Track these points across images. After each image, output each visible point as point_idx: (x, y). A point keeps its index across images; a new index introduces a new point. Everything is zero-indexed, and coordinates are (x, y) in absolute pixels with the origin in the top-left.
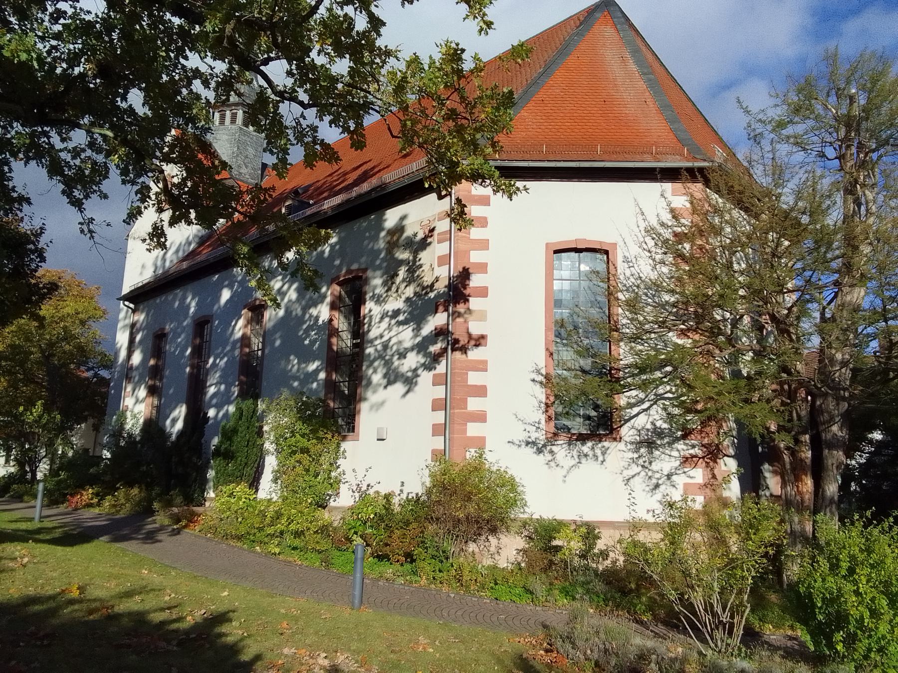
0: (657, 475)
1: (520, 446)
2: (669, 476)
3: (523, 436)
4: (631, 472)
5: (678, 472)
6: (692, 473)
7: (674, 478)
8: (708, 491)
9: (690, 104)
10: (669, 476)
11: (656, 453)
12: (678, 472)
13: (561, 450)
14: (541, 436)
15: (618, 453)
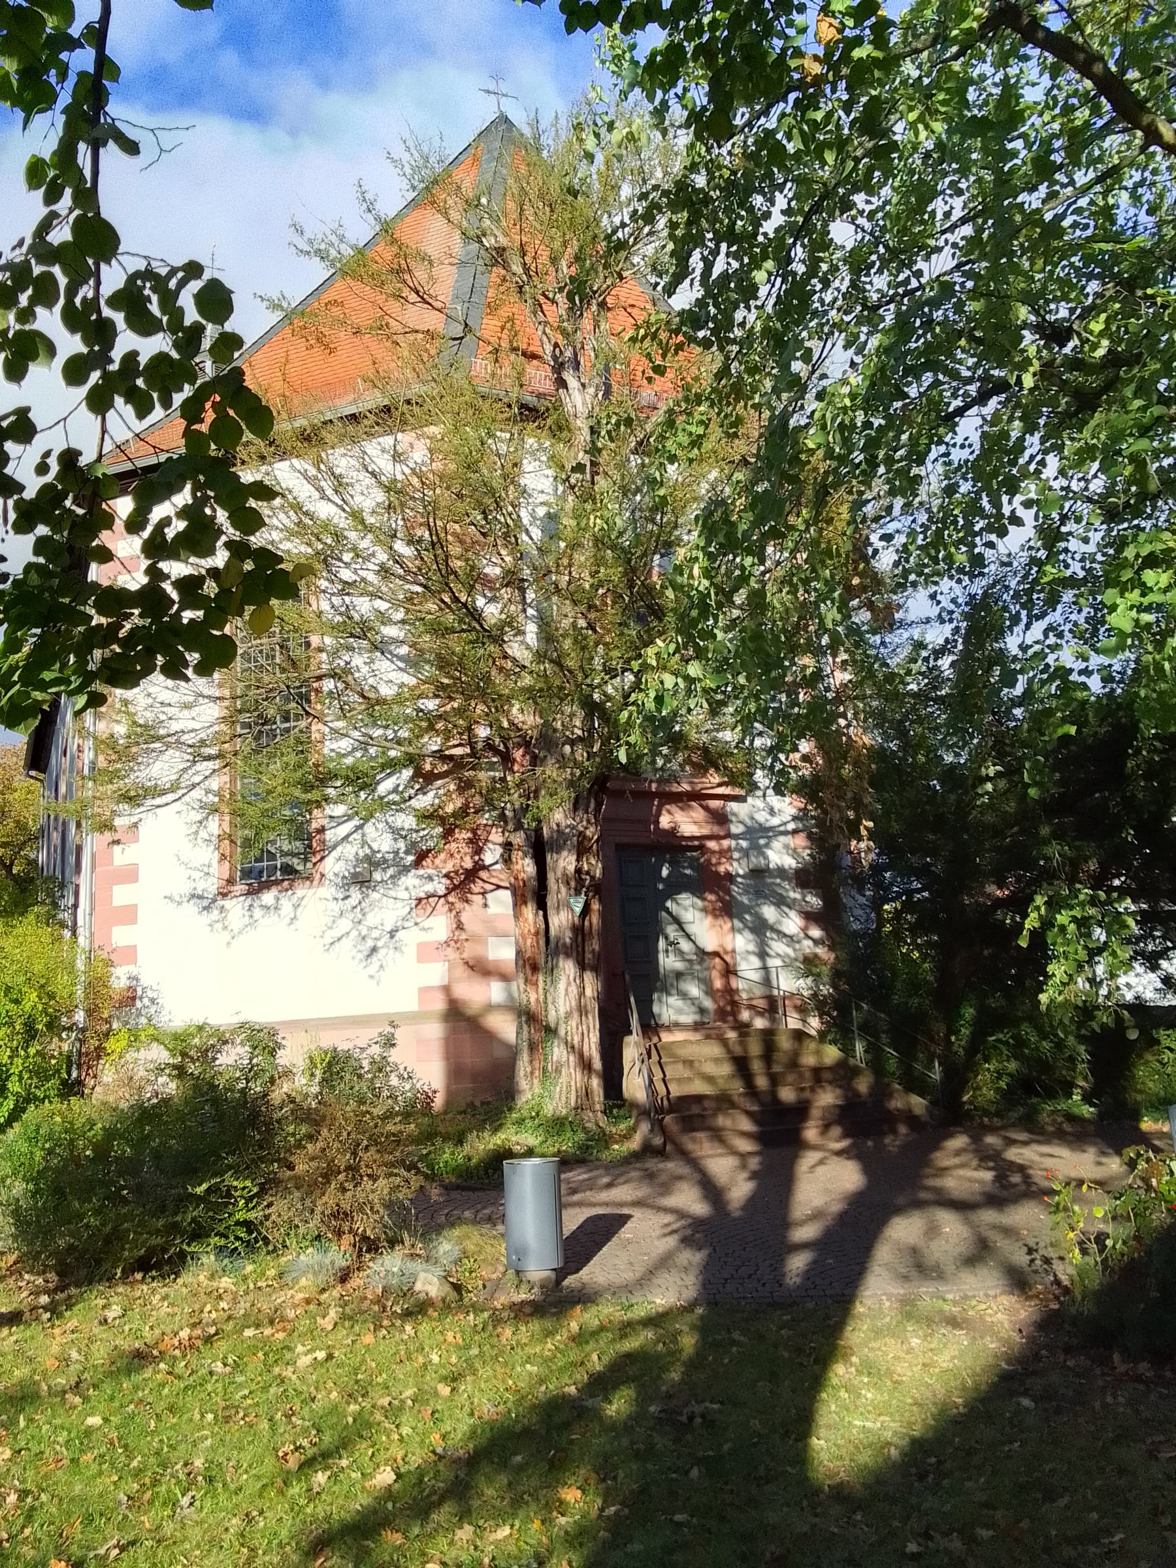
0: (376, 933)
1: (180, 903)
2: (392, 934)
3: (186, 888)
4: (336, 933)
5: (406, 924)
6: (428, 923)
7: (400, 935)
8: (449, 951)
9: (462, 158)
10: (392, 934)
11: (375, 896)
12: (406, 924)
13: (236, 907)
14: (211, 886)
15: (315, 904)
